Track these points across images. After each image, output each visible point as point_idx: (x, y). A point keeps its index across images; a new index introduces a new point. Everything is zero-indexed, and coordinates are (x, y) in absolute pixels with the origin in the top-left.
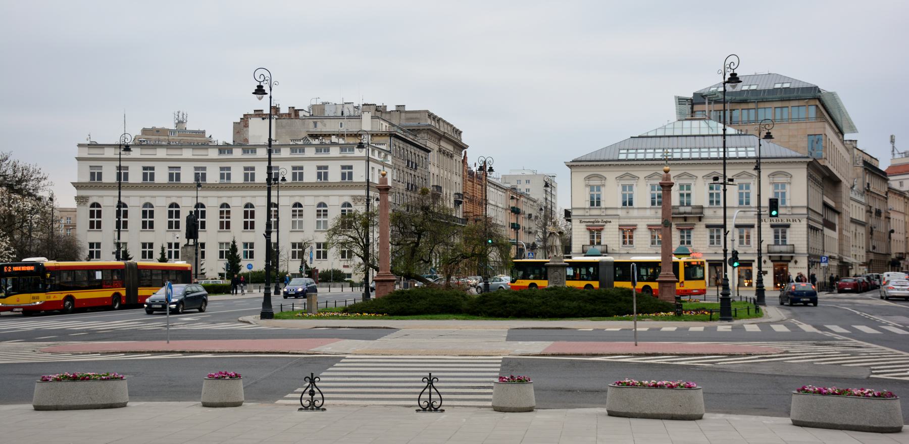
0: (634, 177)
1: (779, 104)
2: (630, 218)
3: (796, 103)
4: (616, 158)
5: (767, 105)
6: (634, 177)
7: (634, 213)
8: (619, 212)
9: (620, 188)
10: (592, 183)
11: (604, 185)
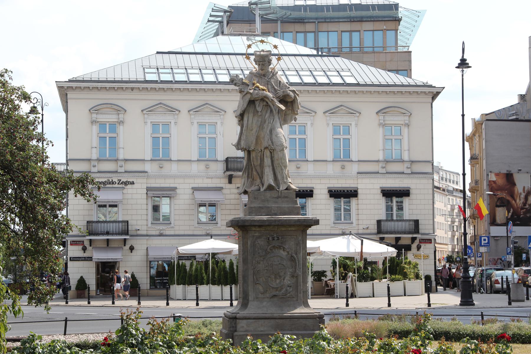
0: (172, 110)
1: (347, 26)
3: (369, 26)
4: (141, 78)
6: (172, 110)
7: (173, 169)
8: (148, 167)
9: (149, 129)
10: (102, 118)
11: (121, 122)
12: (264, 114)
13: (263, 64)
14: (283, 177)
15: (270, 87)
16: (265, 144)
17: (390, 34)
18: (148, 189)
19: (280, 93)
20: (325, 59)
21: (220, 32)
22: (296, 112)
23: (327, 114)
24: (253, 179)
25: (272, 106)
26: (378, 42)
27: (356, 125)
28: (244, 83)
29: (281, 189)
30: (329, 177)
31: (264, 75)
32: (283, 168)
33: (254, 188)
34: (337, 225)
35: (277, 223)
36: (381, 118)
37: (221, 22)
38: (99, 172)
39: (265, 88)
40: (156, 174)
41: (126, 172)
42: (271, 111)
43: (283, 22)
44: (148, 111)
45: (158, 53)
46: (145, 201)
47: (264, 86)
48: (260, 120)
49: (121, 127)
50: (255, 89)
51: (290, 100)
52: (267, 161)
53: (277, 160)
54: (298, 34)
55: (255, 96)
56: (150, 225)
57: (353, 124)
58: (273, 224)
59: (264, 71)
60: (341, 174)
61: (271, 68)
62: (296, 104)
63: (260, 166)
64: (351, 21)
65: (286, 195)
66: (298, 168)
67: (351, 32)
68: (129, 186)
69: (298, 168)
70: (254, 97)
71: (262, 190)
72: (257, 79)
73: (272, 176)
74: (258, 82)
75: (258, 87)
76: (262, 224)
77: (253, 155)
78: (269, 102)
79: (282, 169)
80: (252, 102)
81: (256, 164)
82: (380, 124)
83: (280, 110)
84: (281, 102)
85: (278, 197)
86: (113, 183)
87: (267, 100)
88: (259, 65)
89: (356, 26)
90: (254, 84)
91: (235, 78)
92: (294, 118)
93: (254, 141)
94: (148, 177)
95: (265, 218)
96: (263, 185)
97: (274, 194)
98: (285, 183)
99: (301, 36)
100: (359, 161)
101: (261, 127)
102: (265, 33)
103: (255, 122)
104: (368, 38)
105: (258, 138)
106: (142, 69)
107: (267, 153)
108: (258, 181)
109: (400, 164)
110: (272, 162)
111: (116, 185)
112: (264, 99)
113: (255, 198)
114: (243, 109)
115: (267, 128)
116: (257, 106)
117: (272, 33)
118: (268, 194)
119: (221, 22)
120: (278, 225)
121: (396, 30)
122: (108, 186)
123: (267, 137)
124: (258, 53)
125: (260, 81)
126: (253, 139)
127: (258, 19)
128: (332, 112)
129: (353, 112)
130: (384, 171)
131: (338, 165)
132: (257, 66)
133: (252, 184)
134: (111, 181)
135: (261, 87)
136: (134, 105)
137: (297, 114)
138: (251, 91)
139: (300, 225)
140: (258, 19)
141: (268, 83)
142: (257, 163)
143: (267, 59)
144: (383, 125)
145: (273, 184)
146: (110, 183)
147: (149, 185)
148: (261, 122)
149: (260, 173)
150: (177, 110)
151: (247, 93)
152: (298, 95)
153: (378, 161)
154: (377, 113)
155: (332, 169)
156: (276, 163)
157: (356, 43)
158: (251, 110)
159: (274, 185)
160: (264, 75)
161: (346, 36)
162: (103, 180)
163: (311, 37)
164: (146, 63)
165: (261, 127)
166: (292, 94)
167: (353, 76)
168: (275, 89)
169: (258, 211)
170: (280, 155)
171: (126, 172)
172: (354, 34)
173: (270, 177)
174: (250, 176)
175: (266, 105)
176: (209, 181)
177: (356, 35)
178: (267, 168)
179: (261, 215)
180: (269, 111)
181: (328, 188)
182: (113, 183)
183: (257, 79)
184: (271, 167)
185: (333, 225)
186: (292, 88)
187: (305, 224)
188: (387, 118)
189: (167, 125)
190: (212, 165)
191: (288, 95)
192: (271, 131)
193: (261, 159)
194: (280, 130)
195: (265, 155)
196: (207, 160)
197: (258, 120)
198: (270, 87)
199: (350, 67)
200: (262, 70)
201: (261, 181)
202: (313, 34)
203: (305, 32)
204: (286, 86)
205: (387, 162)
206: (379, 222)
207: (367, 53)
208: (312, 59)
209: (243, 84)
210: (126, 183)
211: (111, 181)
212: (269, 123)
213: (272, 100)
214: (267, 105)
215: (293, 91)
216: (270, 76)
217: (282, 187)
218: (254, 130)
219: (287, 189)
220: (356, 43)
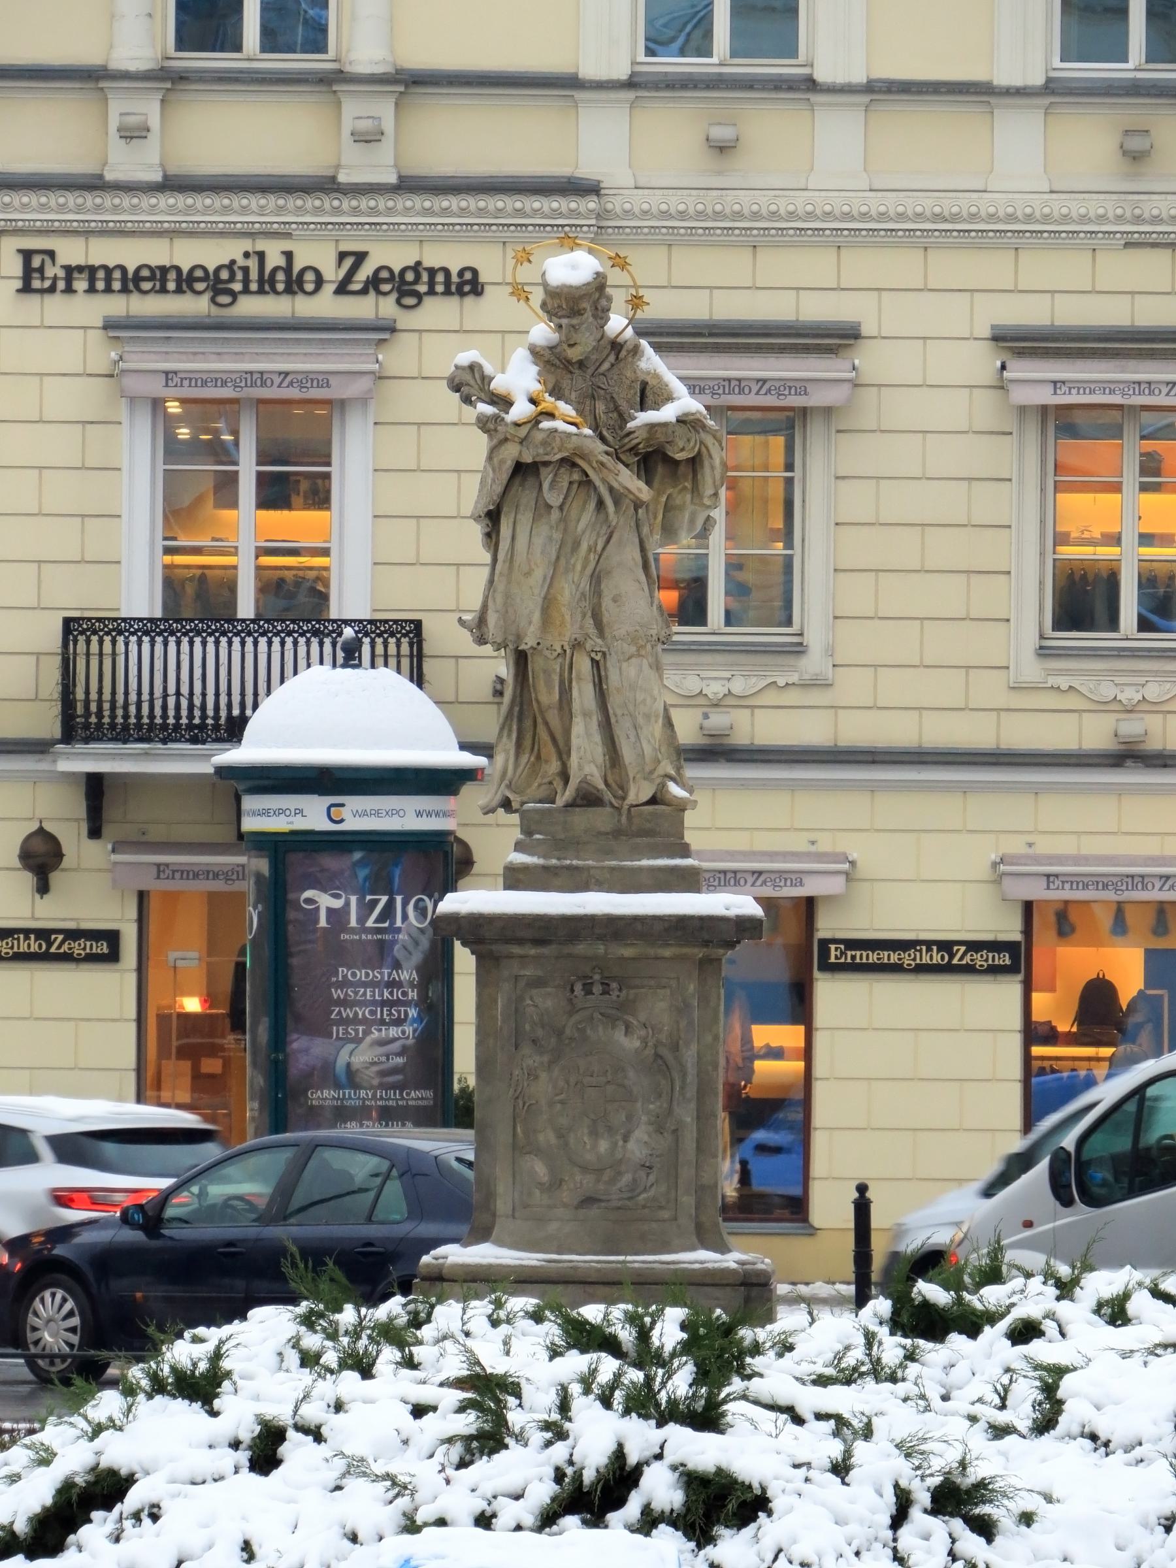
12: (574, 513)
24: (538, 757)
29: (632, 798)
32: (641, 720)
42: (600, 504)
52: (583, 695)
53: (618, 690)
63: (561, 708)
77: (536, 665)
78: (590, 472)
85: (617, 833)
93: (537, 617)
97: (600, 819)
103: (538, 541)
107: (583, 665)
116: (546, 485)
118: (584, 819)
134: (274, 259)
142: (547, 695)
146: (267, 285)
156: (615, 703)
158: (526, 496)
174: (527, 742)
175: (580, 483)
180: (592, 505)
182: (295, 282)
193: (562, 682)
197: (550, 538)
211: (274, 259)
218: (538, 573)
219: (653, 801)
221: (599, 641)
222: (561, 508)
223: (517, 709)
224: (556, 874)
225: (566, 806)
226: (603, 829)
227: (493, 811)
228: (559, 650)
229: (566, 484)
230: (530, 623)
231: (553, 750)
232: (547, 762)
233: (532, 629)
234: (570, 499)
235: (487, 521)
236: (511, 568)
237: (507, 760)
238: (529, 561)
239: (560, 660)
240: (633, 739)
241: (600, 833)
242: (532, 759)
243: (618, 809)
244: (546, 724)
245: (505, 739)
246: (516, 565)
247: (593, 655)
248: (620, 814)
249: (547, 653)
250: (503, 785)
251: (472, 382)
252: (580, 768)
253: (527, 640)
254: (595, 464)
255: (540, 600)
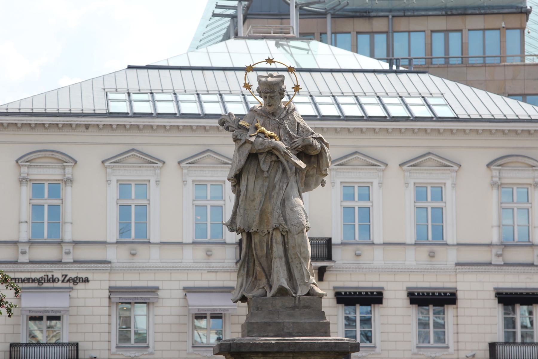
0: (152, 161)
1: (441, 23)
2: (141, 270)
4: (101, 108)
5: (414, 24)
6: (152, 161)
7: (153, 256)
8: (111, 254)
9: (113, 191)
10: (37, 174)
11: (69, 181)
12: (273, 174)
13: (271, 97)
14: (303, 276)
15: (282, 132)
16: (274, 222)
17: (513, 36)
18: (112, 290)
19: (299, 142)
20: (403, 76)
21: (232, 33)
22: (324, 172)
23: (405, 167)
24: (256, 278)
25: (285, 163)
26: (493, 49)
27: (454, 185)
28: (240, 127)
29: (299, 293)
30: (410, 271)
31: (273, 114)
32: (303, 260)
33: (257, 292)
34: (422, 351)
35: (292, 349)
36: (496, 173)
37: (234, 17)
38: (31, 262)
39: (274, 134)
40: (125, 265)
41: (75, 262)
42: (284, 170)
43: (335, 16)
44: (114, 161)
45: (130, 67)
46: (106, 311)
47: (273, 131)
48: (266, 184)
49: (69, 189)
50: (258, 136)
51: (314, 153)
52: (278, 250)
53: (293, 247)
54: (360, 36)
55: (258, 147)
56: (114, 349)
57: (449, 184)
58: (286, 349)
59: (273, 107)
60: (429, 267)
61: (284, 103)
62: (324, 159)
63: (267, 257)
64: (447, 15)
65: (307, 304)
66: (358, 255)
67: (447, 32)
68: (81, 285)
69: (358, 255)
70: (257, 148)
71: (269, 295)
72: (262, 120)
73: (286, 273)
74: (263, 125)
75: (263, 133)
76: (268, 350)
77: (256, 239)
78: (280, 157)
79: (301, 263)
80: (253, 157)
81: (259, 253)
82: (494, 185)
83: (298, 169)
84: (299, 156)
85: (295, 307)
86: (54, 281)
87: (277, 153)
88: (265, 98)
89: (456, 22)
90: (256, 128)
91: (228, 119)
92: (320, 180)
93: (257, 218)
94: (112, 271)
95: (273, 340)
96: (271, 287)
97: (288, 301)
98: (306, 284)
99: (364, 39)
100: (458, 244)
101: (268, 196)
102: (305, 36)
103: (258, 187)
104: (475, 42)
105: (262, 213)
106: (103, 94)
107: (278, 237)
108: (264, 281)
109: (528, 250)
110: (286, 250)
111: (59, 284)
112: (272, 152)
113: (258, 308)
114: (240, 167)
115: (278, 197)
116: (261, 163)
117: (317, 35)
118: (279, 302)
119: (234, 17)
120: (293, 352)
121: (522, 29)
122: (46, 285)
123: (277, 212)
124: (263, 79)
125: (267, 122)
126: (255, 215)
127: (294, 13)
128: (413, 163)
129: (447, 164)
130: (500, 261)
131: (424, 251)
132: (261, 100)
133: (254, 286)
134: (50, 276)
135: (268, 132)
136: (89, 153)
137: (326, 175)
138: (253, 139)
139: (328, 352)
140: (294, 13)
141: (279, 127)
142: (261, 252)
143: (277, 89)
144: (498, 186)
145: (286, 285)
146: (49, 281)
147: (113, 284)
148: (268, 188)
149: (266, 269)
150: (159, 161)
151: (245, 142)
152: (327, 144)
153: (490, 245)
154: (488, 165)
155: (413, 258)
156: (291, 252)
157: (455, 50)
158: (253, 168)
159: (287, 287)
160: (273, 114)
161: (438, 38)
162: (38, 276)
163: (381, 40)
164: (110, 85)
165: (268, 196)
166: (317, 143)
167: (448, 104)
168: (290, 135)
169: (262, 328)
170: (298, 239)
171: (75, 262)
172: (452, 35)
173: (282, 275)
174: (251, 273)
175: (275, 162)
176: (212, 276)
177: (455, 38)
178: (277, 259)
179: (267, 336)
180: (280, 171)
181: (408, 288)
183: (262, 120)
184: (284, 259)
185: (416, 350)
186: (316, 135)
187: (337, 350)
188: (504, 174)
189: (143, 184)
190: (218, 251)
191: (311, 145)
192: (283, 202)
193: (267, 246)
194: (298, 200)
195: (274, 241)
196: (209, 243)
197: (263, 185)
198: (282, 132)
199: (444, 89)
200: (270, 106)
201: (268, 281)
202: (384, 36)
203: (372, 33)
204: (308, 131)
205: (505, 246)
206: (492, 346)
207: (473, 66)
208: (381, 76)
209: (239, 128)
210: (75, 281)
211: (50, 276)
212: (280, 189)
213: (285, 153)
214: (278, 161)
215: (320, 139)
216: (283, 115)
217: (302, 291)
218: (258, 200)
219: (308, 294)
220: (455, 50)
221: (285, 226)
222: (268, 171)
223: (247, 258)
224: (270, 325)
225: (273, 296)
226: (288, 306)
227: (236, 302)
228: (266, 232)
229: (269, 162)
230: (254, 222)
231: (263, 274)
232: (260, 280)
233: (255, 223)
234: (271, 168)
235: (235, 180)
236: (246, 198)
237: (243, 280)
238: (254, 195)
239: (267, 236)
240: (299, 268)
241: (287, 307)
242: (253, 279)
243: (295, 297)
244: (260, 264)
245: (242, 271)
246: (248, 196)
247: (283, 233)
248: (295, 299)
249: (261, 233)
250: (242, 291)
251: (229, 121)
252: (278, 280)
253: (253, 228)
254: (282, 153)
255: (259, 211)
